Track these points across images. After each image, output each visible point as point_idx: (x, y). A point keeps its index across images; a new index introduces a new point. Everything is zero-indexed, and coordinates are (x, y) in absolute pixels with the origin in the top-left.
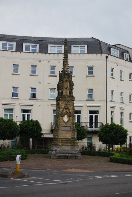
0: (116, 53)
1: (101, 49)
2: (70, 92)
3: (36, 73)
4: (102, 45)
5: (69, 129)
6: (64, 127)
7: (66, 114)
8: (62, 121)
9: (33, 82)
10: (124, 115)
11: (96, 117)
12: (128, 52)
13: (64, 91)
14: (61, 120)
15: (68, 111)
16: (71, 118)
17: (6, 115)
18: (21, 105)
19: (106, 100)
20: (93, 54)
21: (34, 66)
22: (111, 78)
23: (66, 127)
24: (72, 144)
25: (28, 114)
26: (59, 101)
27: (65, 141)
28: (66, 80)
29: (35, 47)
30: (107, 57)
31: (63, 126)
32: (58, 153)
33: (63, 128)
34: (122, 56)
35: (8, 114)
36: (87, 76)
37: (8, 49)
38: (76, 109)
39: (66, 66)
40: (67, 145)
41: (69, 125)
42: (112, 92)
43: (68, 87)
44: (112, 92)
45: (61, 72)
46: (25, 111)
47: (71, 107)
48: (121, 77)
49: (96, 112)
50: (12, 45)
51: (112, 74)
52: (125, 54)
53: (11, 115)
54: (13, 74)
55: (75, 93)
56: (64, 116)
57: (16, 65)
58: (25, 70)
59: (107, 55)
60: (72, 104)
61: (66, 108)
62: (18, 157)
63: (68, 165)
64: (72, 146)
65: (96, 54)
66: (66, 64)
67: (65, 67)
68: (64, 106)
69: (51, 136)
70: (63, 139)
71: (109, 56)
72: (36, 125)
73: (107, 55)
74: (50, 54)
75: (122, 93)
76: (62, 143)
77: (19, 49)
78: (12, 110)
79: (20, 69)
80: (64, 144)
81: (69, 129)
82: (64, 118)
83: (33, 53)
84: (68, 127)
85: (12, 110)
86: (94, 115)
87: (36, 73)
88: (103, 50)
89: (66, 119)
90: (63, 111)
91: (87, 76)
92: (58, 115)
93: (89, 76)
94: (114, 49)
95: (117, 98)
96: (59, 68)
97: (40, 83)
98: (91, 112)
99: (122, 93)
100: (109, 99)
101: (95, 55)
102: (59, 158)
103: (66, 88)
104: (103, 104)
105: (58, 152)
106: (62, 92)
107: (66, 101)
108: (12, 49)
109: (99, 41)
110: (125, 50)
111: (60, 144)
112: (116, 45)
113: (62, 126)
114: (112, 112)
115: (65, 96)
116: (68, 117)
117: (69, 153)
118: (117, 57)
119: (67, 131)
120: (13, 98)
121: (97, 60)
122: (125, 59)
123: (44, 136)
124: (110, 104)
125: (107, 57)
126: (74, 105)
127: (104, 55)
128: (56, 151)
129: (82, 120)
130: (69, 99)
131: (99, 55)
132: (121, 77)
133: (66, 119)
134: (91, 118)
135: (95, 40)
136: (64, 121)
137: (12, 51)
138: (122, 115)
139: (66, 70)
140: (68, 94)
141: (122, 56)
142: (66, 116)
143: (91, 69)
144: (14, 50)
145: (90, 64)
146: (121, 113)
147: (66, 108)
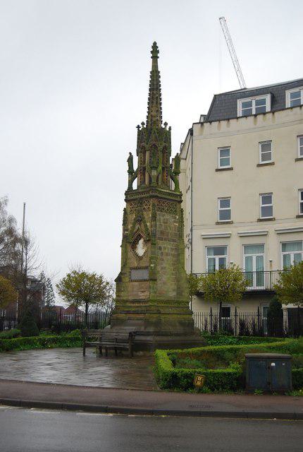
7: (139, 237)
17: (249, 260)
18: (280, 233)
41: (144, 265)
47: (148, 215)
50: (263, 102)
57: (266, 146)
70: (133, 302)
76: (128, 312)
78: (261, 247)
79: (273, 150)
85: (261, 247)
90: (134, 227)
133: (141, 249)
142: (141, 241)
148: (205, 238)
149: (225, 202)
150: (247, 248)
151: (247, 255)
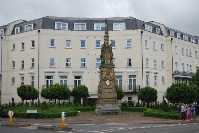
0: (149, 28)
1: (137, 26)
2: (110, 61)
3: (84, 47)
4: (138, 22)
5: (110, 91)
6: (106, 90)
7: (108, 79)
9: (83, 54)
10: (158, 79)
11: (135, 80)
12: (159, 27)
13: (106, 61)
14: (104, 84)
16: (112, 82)
17: (61, 81)
18: (73, 73)
19: (142, 66)
20: (48, 30)
21: (69, 41)
22: (146, 48)
24: (113, 103)
25: (79, 79)
26: (101, 69)
27: (108, 101)
28: (107, 52)
29: (65, 25)
30: (142, 32)
32: (103, 110)
33: (106, 90)
34: (154, 31)
35: (64, 80)
36: (126, 48)
37: (61, 29)
38: (116, 74)
39: (107, 40)
40: (109, 104)
42: (147, 60)
43: (109, 57)
44: (147, 60)
45: (103, 46)
46: (49, 77)
48: (154, 47)
49: (135, 76)
51: (146, 46)
52: (157, 29)
53: (66, 81)
54: (66, 48)
55: (115, 62)
56: (106, 80)
58: (76, 44)
59: (142, 30)
60: (113, 70)
61: (108, 74)
62: (63, 114)
63: (109, 120)
64: (113, 104)
65: (133, 30)
66: (107, 39)
67: (106, 41)
68: (106, 73)
69: (97, 97)
71: (144, 31)
72: (85, 89)
73: (142, 30)
74: (95, 31)
75: (155, 61)
76: (105, 102)
77: (71, 28)
78: (66, 77)
79: (72, 43)
80: (107, 103)
81: (110, 91)
82: (106, 82)
83: (82, 31)
85: (66, 77)
86: (132, 79)
87: (84, 47)
88: (139, 26)
89: (108, 83)
90: (105, 76)
91: (126, 48)
92: (102, 80)
93: (128, 48)
94: (148, 26)
95: (151, 65)
96: (102, 43)
97: (88, 55)
98: (130, 76)
99: (155, 61)
100: (145, 66)
101: (132, 31)
102: (103, 114)
103: (107, 58)
104: (140, 70)
105: (101, 110)
106: (104, 62)
107: (108, 68)
108: (65, 28)
109: (136, 19)
110: (157, 26)
111: (104, 103)
112: (149, 22)
114: (147, 76)
115: (106, 64)
117: (111, 110)
118: (150, 32)
120: (67, 68)
121: (134, 34)
122: (157, 33)
123: (91, 97)
124: (145, 70)
125: (142, 32)
126: (114, 72)
127: (139, 31)
128: (100, 108)
129: (123, 83)
131: (135, 30)
132: (154, 47)
133: (108, 83)
134: (130, 80)
135: (132, 18)
136: (106, 84)
137: (65, 30)
138: (156, 78)
139: (107, 43)
140: (109, 63)
141: (154, 31)
142: (108, 80)
143: (129, 41)
144: (67, 28)
145: (128, 38)
146: (155, 77)
147: (108, 74)
148: (45, 72)
149: (52, 60)
150: (61, 77)
151: (61, 80)
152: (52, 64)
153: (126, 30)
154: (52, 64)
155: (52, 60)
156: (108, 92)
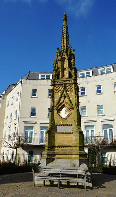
7: (63, 106)
8: (58, 117)
15: (67, 99)
23: (65, 127)
31: (60, 125)
41: (69, 124)
56: (61, 109)
61: (63, 96)
70: (59, 146)
81: (69, 129)
84: (68, 127)
113: (58, 125)
116: (68, 109)
119: (67, 133)
130: (67, 83)
133: (64, 113)
142: (64, 109)
152: (33, 114)
153: (113, 73)
154: (33, 114)
155: (33, 109)
156: (63, 133)
